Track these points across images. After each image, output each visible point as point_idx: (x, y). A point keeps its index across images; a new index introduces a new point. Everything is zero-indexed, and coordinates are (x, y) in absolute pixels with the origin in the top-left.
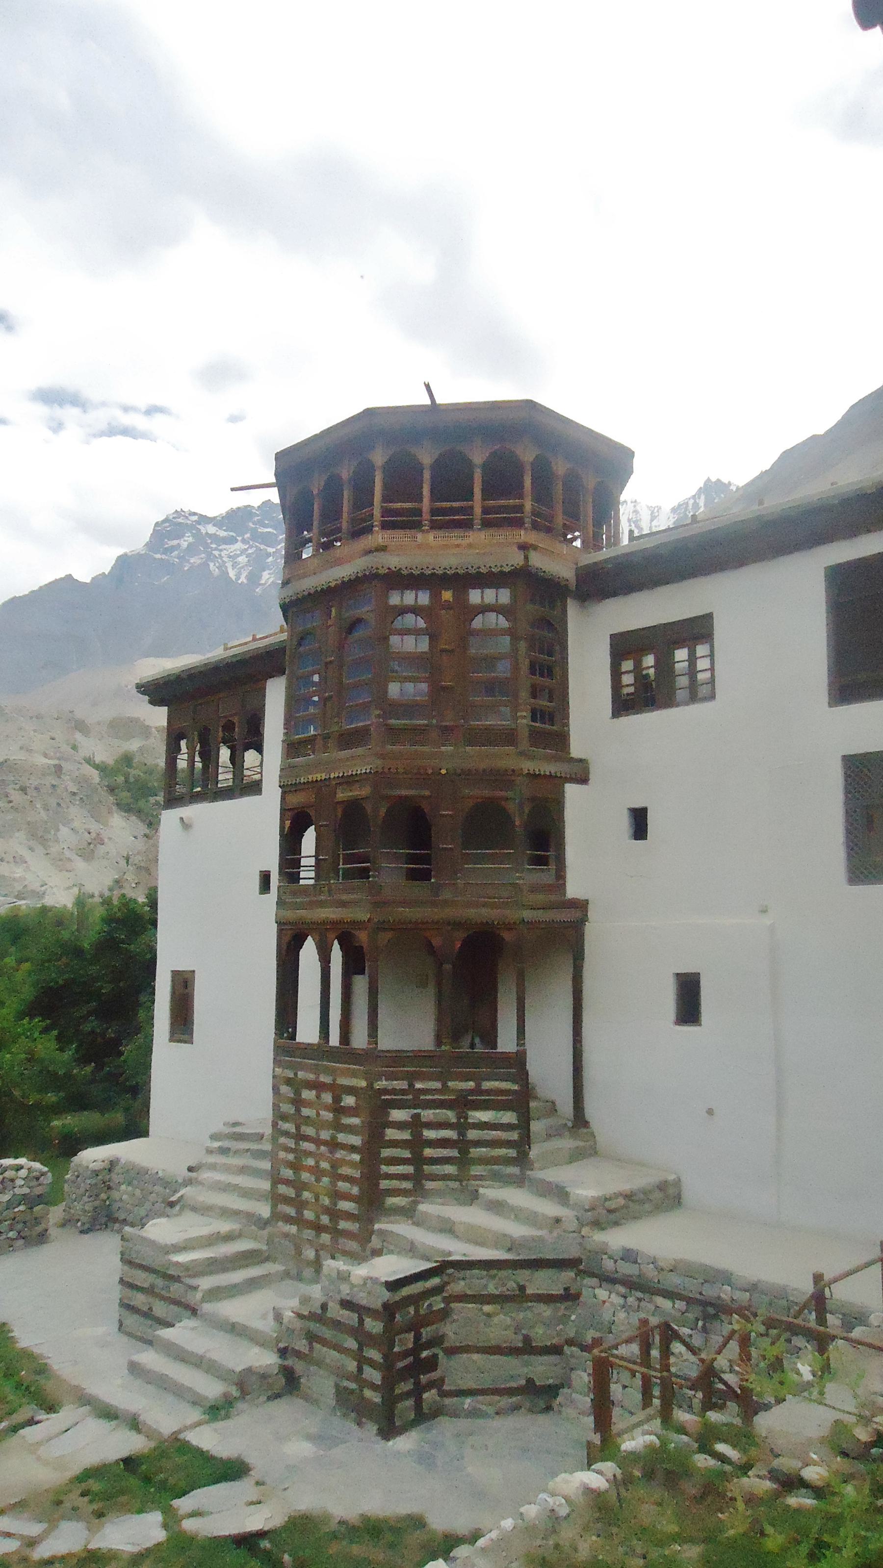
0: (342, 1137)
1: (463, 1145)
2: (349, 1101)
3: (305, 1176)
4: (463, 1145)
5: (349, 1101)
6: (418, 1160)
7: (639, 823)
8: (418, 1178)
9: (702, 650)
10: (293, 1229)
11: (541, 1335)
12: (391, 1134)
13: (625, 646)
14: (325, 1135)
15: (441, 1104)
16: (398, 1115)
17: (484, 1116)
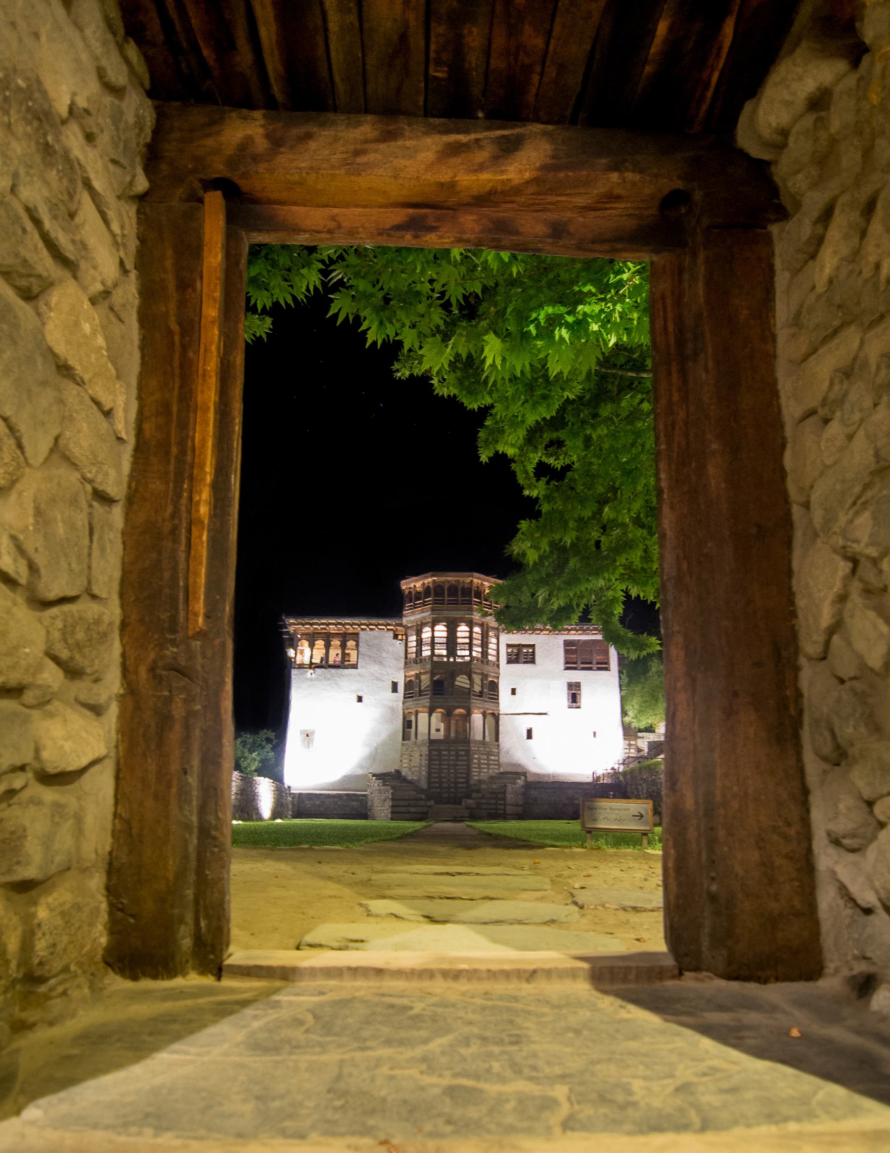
0: (459, 763)
1: (488, 765)
2: (463, 753)
3: (443, 775)
4: (488, 765)
5: (463, 753)
6: (479, 768)
7: (514, 692)
8: (479, 773)
9: (530, 650)
10: (438, 790)
11: (520, 803)
12: (475, 761)
13: (509, 646)
14: (452, 763)
15: (483, 754)
16: (476, 756)
17: (493, 758)
